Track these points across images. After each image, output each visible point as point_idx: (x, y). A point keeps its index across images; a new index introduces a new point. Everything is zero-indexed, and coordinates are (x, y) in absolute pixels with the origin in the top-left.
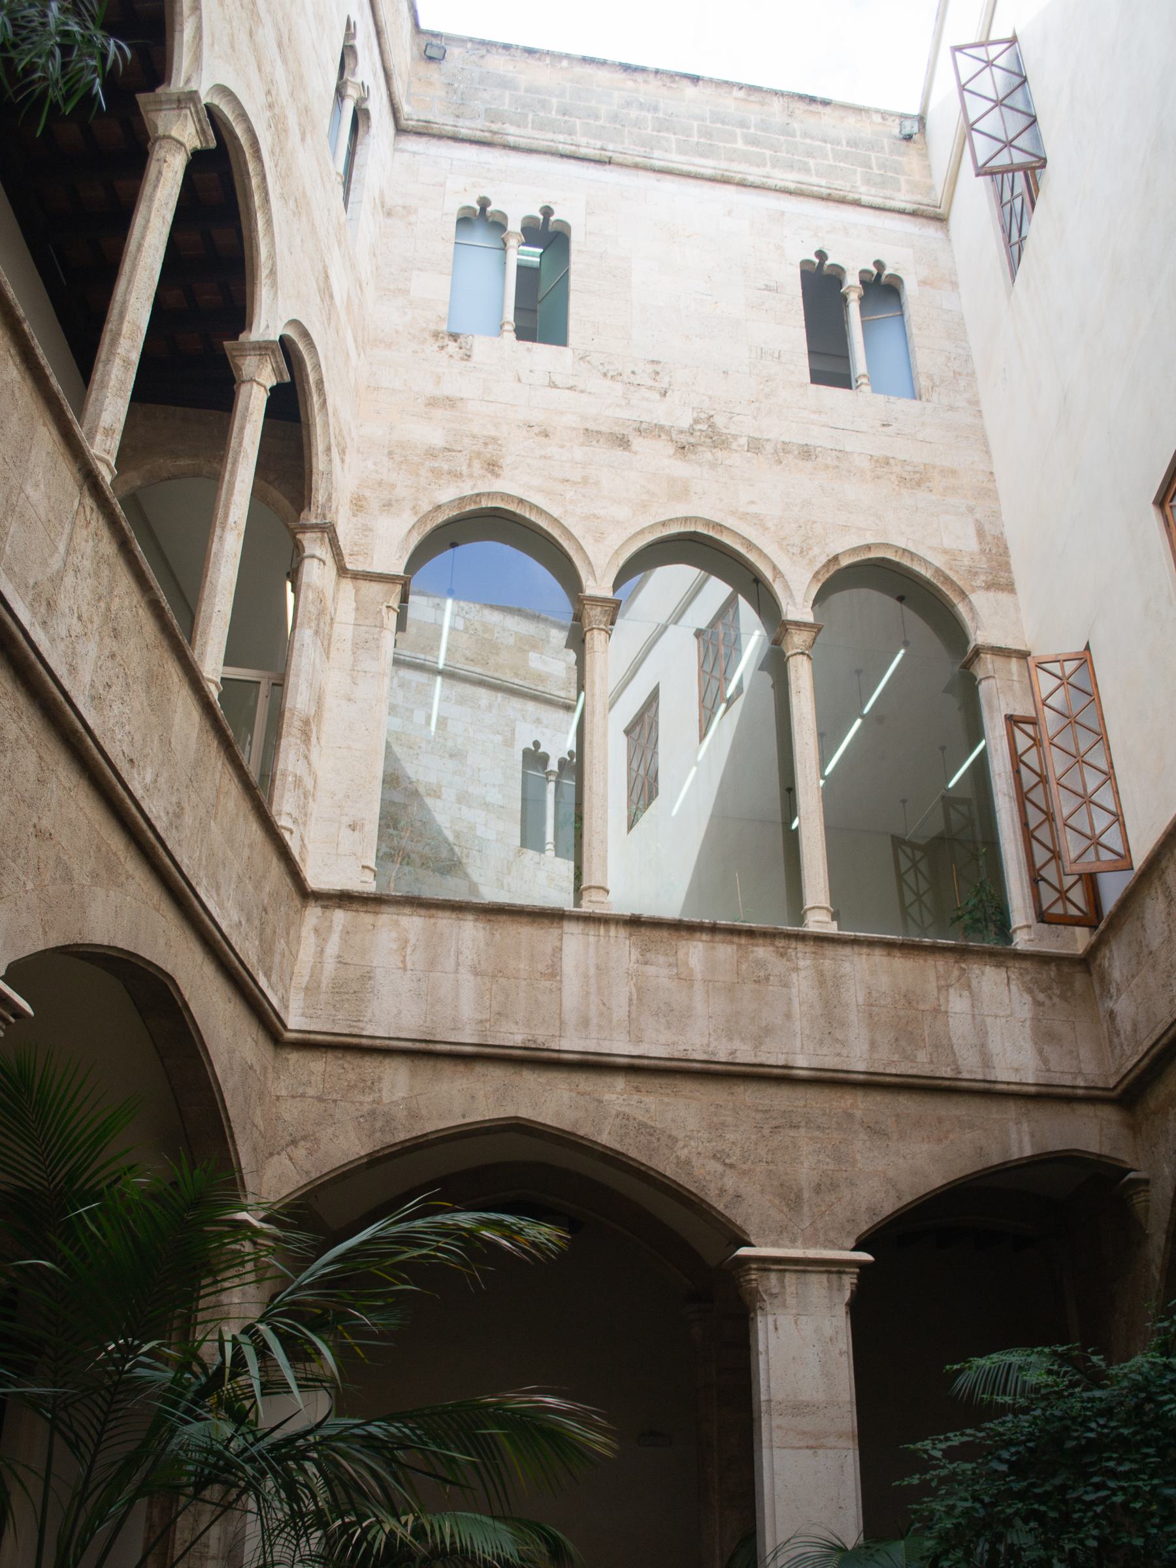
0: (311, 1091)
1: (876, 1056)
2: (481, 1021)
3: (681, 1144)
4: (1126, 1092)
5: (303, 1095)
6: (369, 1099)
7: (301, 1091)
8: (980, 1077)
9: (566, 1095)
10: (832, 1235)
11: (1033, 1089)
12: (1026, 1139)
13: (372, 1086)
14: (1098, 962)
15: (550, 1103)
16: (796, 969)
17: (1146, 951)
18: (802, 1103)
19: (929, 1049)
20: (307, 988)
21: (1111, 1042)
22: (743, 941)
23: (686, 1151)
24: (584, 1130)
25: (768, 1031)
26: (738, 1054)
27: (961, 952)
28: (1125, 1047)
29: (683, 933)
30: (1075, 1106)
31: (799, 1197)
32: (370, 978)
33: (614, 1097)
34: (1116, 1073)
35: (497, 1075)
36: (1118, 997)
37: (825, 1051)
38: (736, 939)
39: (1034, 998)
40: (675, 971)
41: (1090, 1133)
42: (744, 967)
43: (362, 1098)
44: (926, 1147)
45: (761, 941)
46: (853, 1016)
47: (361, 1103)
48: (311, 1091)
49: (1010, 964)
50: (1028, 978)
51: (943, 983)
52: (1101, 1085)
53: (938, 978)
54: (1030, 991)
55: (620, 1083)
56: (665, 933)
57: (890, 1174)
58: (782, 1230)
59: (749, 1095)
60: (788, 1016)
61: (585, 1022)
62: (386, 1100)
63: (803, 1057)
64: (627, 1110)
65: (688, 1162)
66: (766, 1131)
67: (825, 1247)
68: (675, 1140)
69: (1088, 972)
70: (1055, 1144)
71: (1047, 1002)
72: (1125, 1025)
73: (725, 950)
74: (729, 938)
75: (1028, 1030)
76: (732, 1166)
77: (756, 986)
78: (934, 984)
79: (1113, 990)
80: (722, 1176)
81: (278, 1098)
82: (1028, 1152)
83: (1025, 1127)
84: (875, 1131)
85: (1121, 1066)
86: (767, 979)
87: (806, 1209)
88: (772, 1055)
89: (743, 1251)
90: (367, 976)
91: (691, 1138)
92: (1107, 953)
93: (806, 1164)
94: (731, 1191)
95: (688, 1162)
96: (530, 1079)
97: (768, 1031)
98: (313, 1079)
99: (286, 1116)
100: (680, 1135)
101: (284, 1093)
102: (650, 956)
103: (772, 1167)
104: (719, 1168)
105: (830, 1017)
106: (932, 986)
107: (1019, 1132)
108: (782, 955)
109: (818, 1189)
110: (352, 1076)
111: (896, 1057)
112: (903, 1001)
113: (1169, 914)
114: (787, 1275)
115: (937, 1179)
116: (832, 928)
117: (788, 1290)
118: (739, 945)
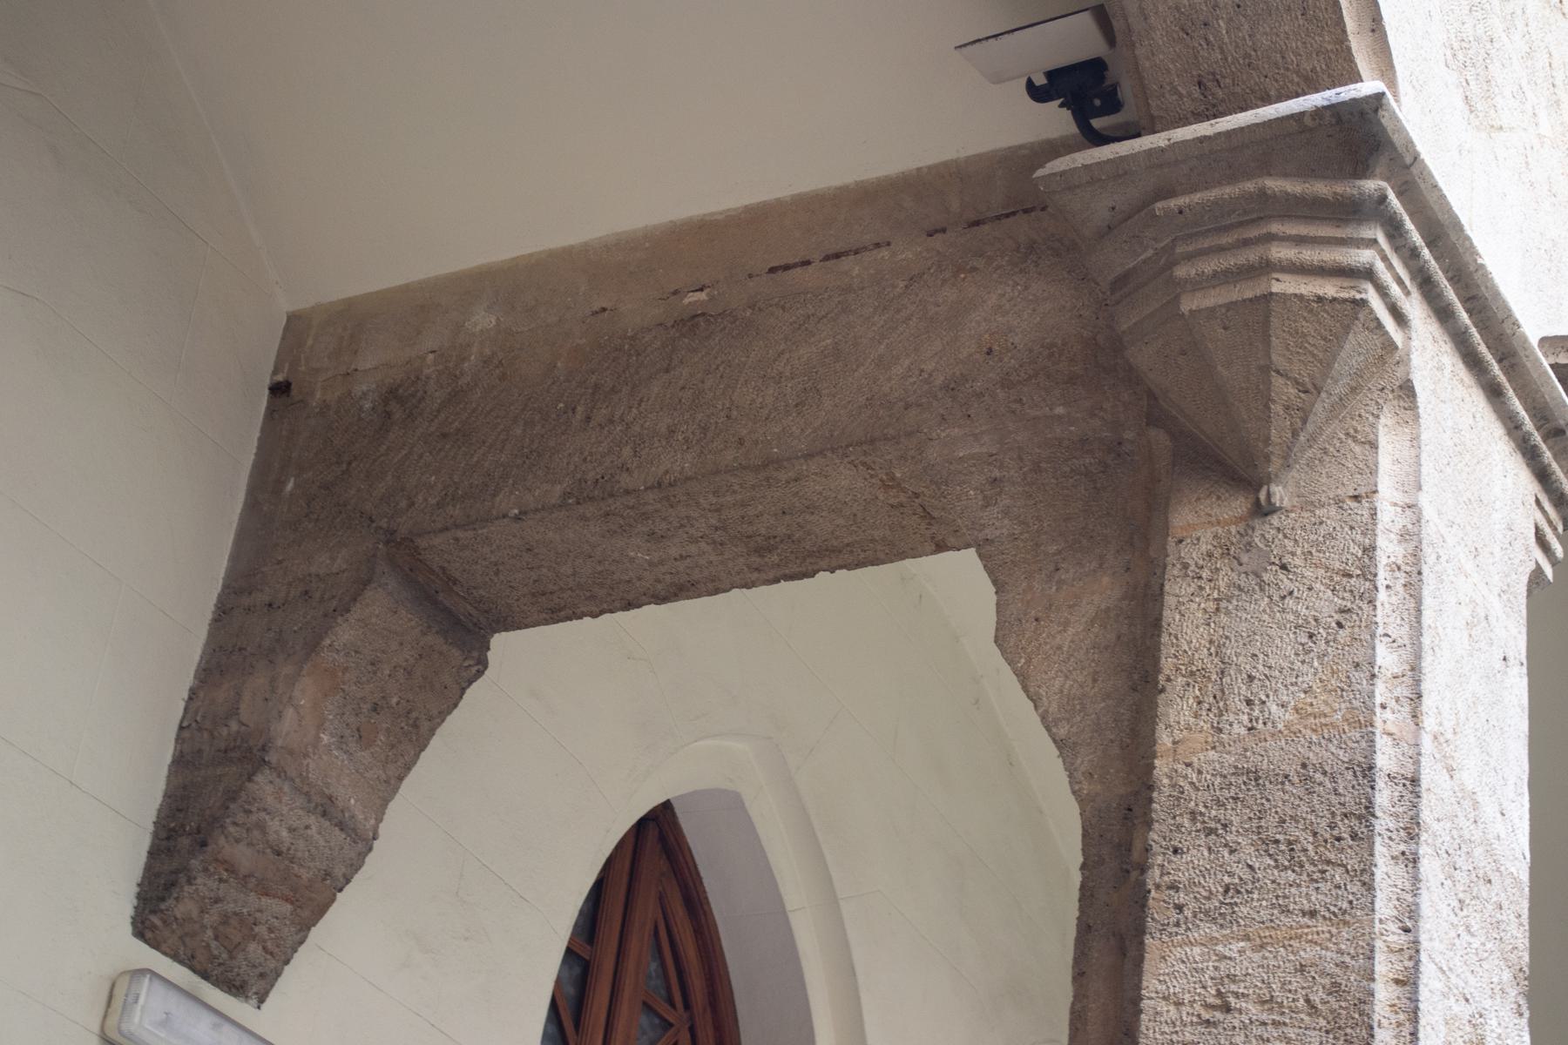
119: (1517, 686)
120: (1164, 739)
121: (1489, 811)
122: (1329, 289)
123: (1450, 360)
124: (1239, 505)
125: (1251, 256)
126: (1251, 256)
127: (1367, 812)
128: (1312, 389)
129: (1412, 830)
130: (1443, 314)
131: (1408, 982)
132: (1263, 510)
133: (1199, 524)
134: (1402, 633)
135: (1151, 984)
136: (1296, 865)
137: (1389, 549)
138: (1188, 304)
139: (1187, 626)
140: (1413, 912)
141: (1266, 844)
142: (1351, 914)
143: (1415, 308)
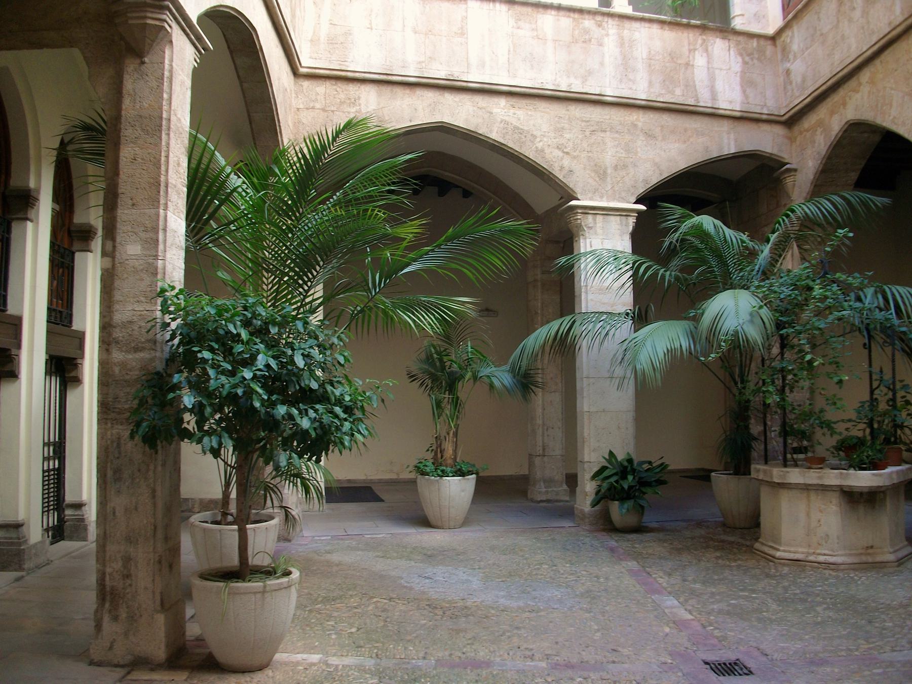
0: (318, 106)
1: (652, 90)
2: (420, 63)
3: (538, 139)
4: (791, 118)
5: (313, 108)
6: (353, 110)
7: (312, 105)
8: (710, 105)
9: (471, 109)
10: (623, 194)
11: (738, 114)
12: (732, 143)
13: (354, 102)
14: (782, 39)
15: (461, 113)
16: (607, 35)
17: (818, 33)
18: (608, 117)
19: (682, 87)
20: (312, 41)
21: (785, 88)
22: (576, 16)
23: (541, 144)
24: (482, 131)
25: (590, 73)
26: (573, 86)
27: (703, 28)
28: (795, 91)
29: (541, 10)
30: (760, 124)
31: (605, 172)
32: (350, 34)
33: (499, 110)
34: (786, 106)
35: (430, 96)
36: (794, 61)
37: (623, 86)
38: (572, 15)
39: (743, 59)
40: (535, 34)
41: (766, 141)
42: (577, 32)
43: (349, 109)
44: (677, 145)
45: (587, 17)
46: (640, 66)
47: (349, 113)
48: (318, 106)
49: (731, 37)
50: (740, 47)
51: (692, 47)
52: (776, 113)
53: (689, 44)
54: (741, 55)
55: (502, 101)
56: (529, 10)
57: (657, 160)
58: (595, 191)
59: (577, 111)
60: (602, 64)
61: (482, 65)
62: (363, 111)
63: (610, 91)
64: (507, 118)
65: (542, 151)
66: (587, 133)
67: (619, 201)
68: (535, 137)
69: (775, 45)
70: (748, 147)
71: (750, 62)
72: (796, 78)
73: (566, 21)
74: (568, 14)
75: (738, 79)
76: (567, 153)
77: (584, 45)
78: (687, 47)
79: (791, 57)
80: (562, 159)
81: (298, 109)
82: (733, 150)
83: (732, 136)
84: (649, 135)
85: (791, 102)
86: (590, 41)
87: (609, 179)
88: (592, 88)
89: (573, 203)
90: (348, 33)
91: (544, 136)
92: (790, 34)
93: (610, 154)
94: (567, 168)
95: (542, 151)
96: (449, 98)
97: (590, 73)
98: (319, 97)
99: (304, 121)
100: (538, 133)
101: (301, 106)
102: (521, 23)
103: (590, 154)
104: (561, 154)
105: (626, 66)
106: (685, 50)
107: (729, 138)
108: (599, 26)
109: (616, 168)
110: (342, 96)
111: (663, 92)
112: (668, 58)
113: (839, 11)
114: (598, 216)
115: (681, 164)
116: (628, 10)
117: (598, 225)
118: (574, 19)
119: (189, 93)
120: (124, 107)
121: (183, 120)
122: (157, 23)
123: (180, 32)
124: (138, 61)
125: (142, 14)
126: (142, 14)
127: (161, 126)
128: (153, 41)
129: (169, 128)
130: (179, 23)
131: (167, 157)
132: (143, 63)
133: (130, 66)
134: (168, 91)
135: (122, 154)
136: (148, 134)
137: (166, 74)
138: (130, 22)
139: (129, 84)
140: (168, 144)
141: (143, 130)
142: (158, 145)
143: (174, 24)
